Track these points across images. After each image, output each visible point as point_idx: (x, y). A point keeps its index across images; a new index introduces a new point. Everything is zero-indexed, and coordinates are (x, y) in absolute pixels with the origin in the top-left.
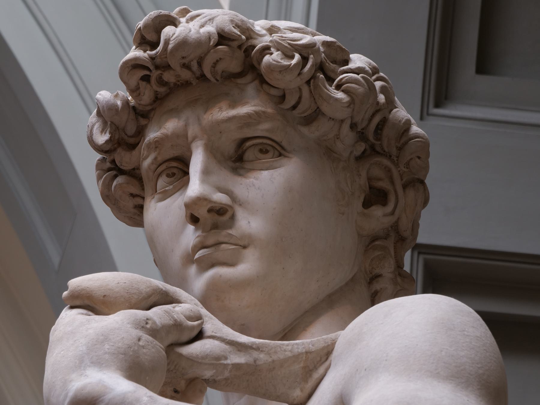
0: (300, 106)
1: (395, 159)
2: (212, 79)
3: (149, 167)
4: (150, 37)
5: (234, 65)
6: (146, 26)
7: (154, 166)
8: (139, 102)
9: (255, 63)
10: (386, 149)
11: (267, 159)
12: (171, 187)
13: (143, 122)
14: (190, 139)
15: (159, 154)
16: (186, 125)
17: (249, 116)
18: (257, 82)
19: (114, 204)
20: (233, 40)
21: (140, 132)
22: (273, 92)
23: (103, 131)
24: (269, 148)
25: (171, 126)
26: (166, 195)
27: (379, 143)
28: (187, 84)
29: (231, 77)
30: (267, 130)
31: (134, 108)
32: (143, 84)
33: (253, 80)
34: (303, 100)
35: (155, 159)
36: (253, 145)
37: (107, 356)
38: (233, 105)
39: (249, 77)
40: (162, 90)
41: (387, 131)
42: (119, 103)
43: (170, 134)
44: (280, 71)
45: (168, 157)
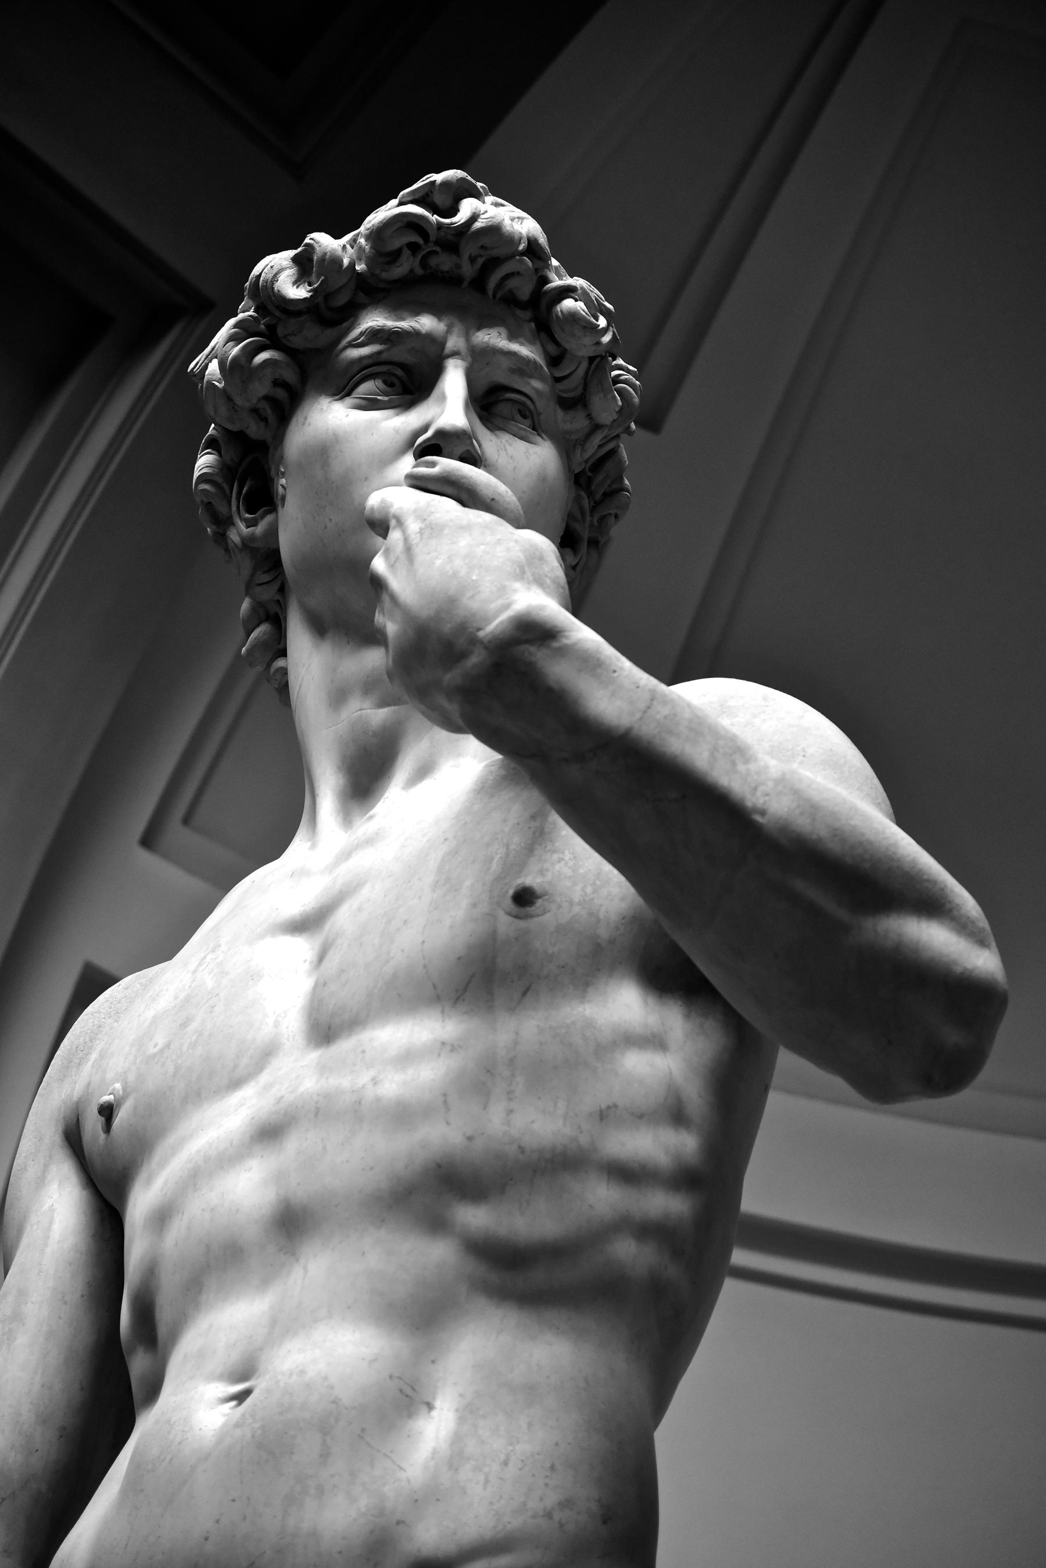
0: (566, 382)
1: (592, 504)
2: (490, 293)
3: (361, 359)
4: (439, 199)
5: (524, 290)
6: (446, 184)
7: (370, 361)
8: (377, 272)
9: (544, 302)
10: (593, 487)
11: (524, 426)
12: (386, 398)
13: (361, 297)
14: (447, 351)
15: (388, 350)
16: (449, 331)
17: (526, 361)
18: (533, 325)
19: (243, 382)
20: (540, 258)
21: (351, 312)
22: (552, 348)
23: (297, 283)
24: (528, 413)
25: (426, 323)
26: (370, 404)
27: (590, 474)
28: (453, 280)
29: (511, 301)
30: (537, 391)
31: (359, 275)
32: (406, 252)
33: (530, 321)
34: (573, 376)
35: (379, 353)
36: (511, 400)
37: (548, 581)
38: (512, 337)
39: (528, 314)
40: (419, 271)
41: (609, 466)
42: (346, 262)
43: (424, 332)
44: (585, 327)
45: (396, 359)
